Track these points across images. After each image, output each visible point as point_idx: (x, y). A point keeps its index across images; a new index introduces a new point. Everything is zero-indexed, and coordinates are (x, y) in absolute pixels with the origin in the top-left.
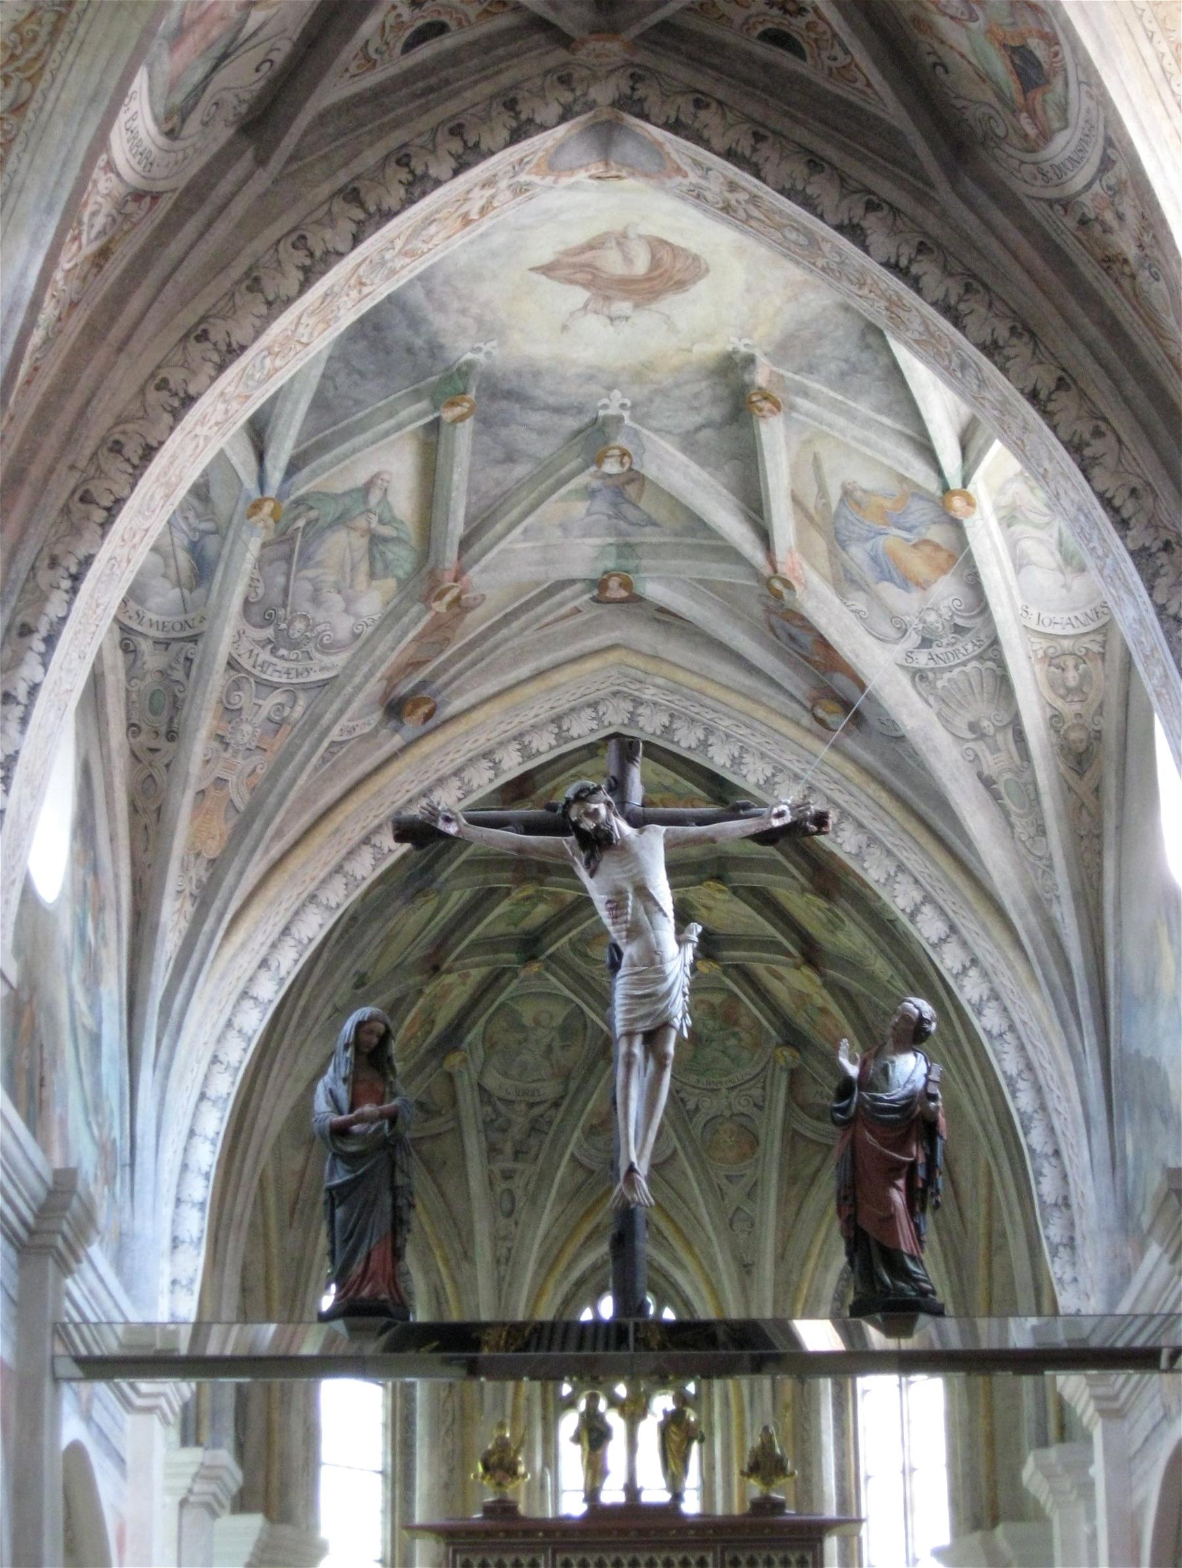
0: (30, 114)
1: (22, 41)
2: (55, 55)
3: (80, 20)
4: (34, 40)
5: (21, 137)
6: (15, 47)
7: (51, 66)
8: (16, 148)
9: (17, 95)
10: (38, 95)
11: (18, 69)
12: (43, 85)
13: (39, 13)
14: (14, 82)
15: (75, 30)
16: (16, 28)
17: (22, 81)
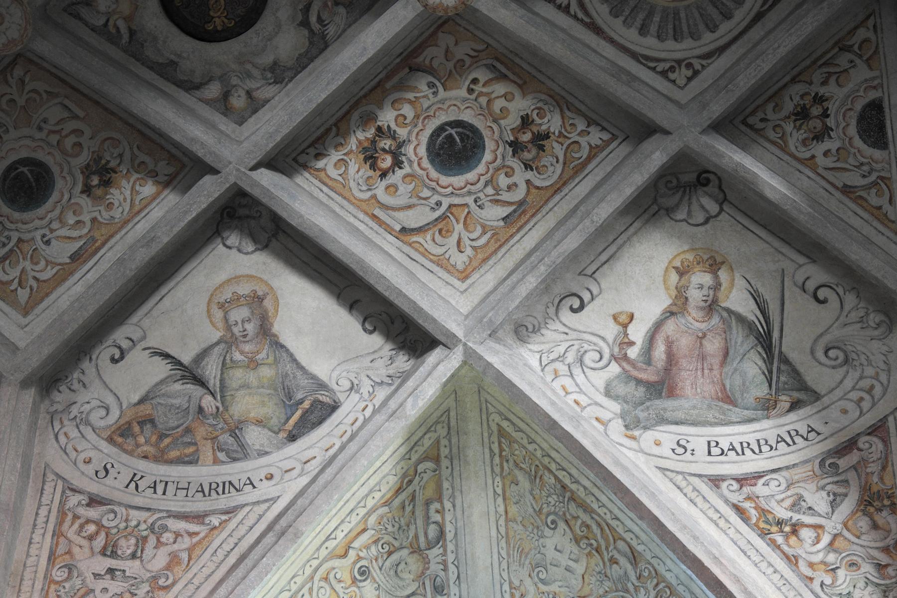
0: (640, 548)
1: (587, 538)
2: (601, 511)
3: (577, 482)
4: (588, 527)
5: (654, 562)
6: (591, 545)
7: (608, 517)
8: (661, 569)
9: (625, 556)
10: (627, 536)
11: (607, 548)
12: (620, 530)
13: (568, 517)
14: (617, 556)
15: (585, 488)
16: (577, 540)
17: (615, 548)
